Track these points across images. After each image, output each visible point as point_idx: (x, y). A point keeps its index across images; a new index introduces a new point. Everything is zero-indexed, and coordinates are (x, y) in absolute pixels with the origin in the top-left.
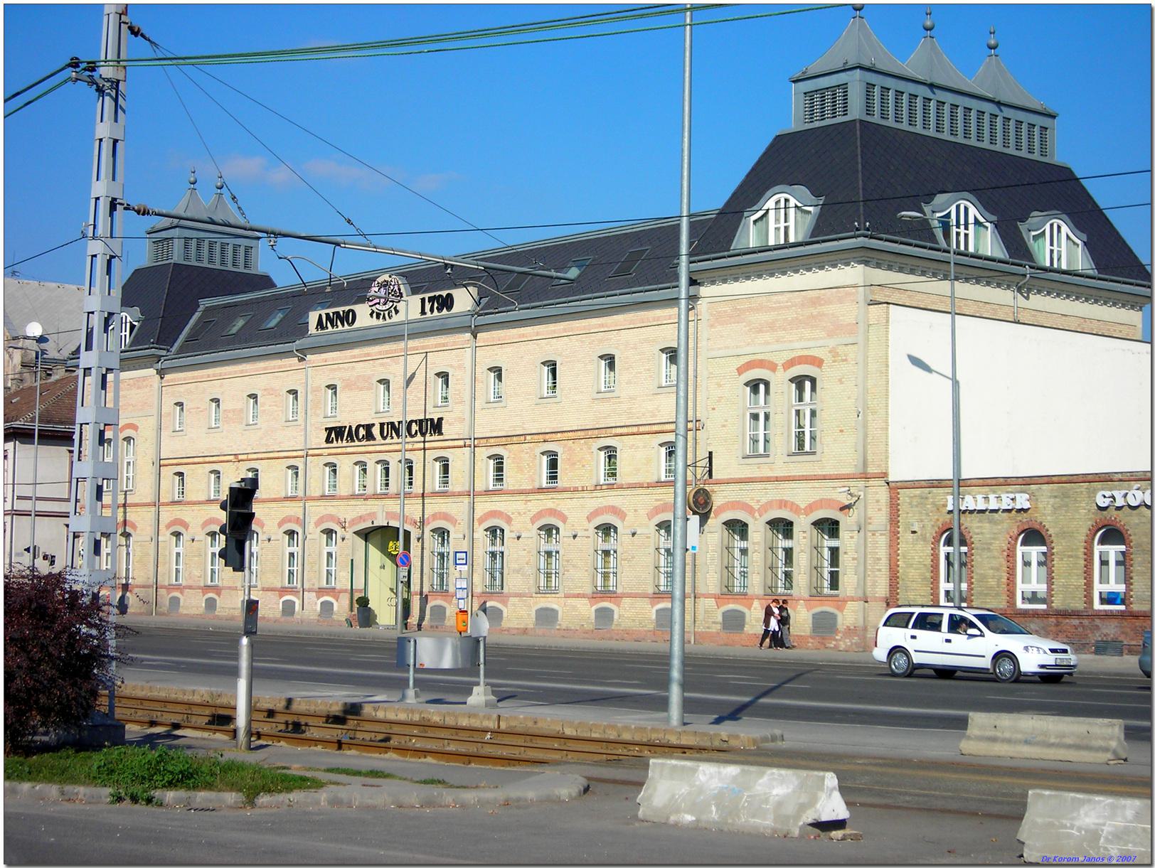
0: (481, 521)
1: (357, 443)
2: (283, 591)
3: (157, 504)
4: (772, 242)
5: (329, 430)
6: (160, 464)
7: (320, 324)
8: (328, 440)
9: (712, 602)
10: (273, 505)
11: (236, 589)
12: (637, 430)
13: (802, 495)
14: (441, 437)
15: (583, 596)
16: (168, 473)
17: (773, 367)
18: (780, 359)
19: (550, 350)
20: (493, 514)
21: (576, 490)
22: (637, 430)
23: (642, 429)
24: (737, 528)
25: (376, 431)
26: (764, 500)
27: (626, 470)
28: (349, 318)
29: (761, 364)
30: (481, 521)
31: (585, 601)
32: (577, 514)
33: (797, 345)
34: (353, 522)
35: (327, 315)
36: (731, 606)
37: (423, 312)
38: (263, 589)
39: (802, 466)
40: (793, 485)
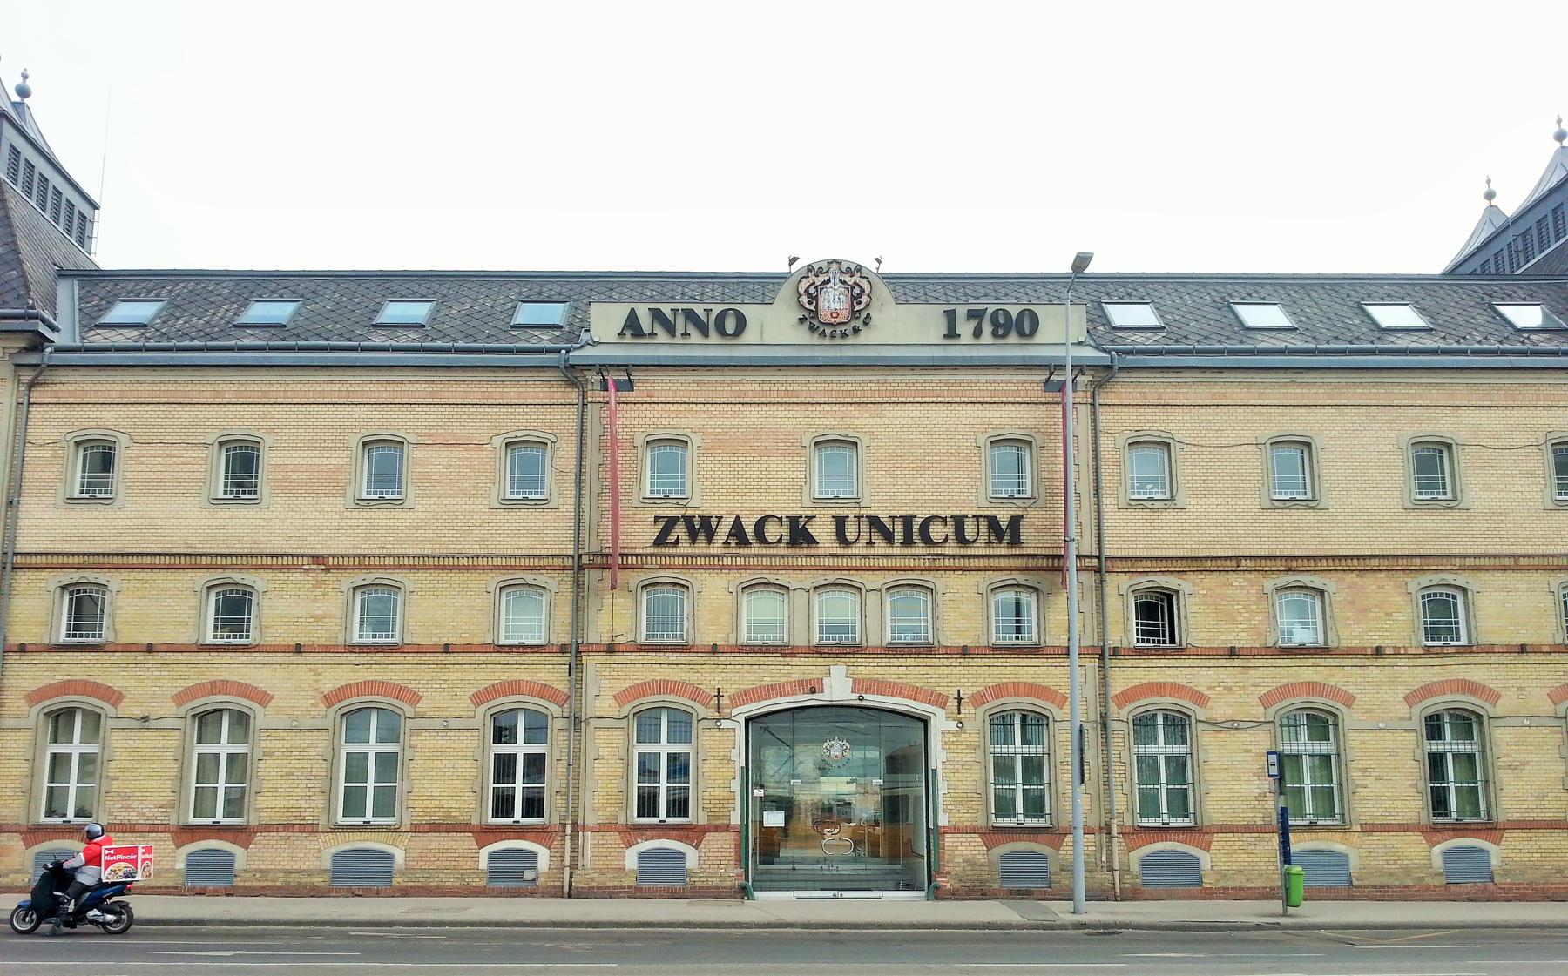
1: (756, 549)
8: (660, 541)
11: (310, 829)
12: (1513, 563)
14: (1017, 551)
15: (1405, 828)
22: (1513, 563)
23: (1522, 561)
25: (822, 531)
30: (1126, 697)
34: (743, 697)
35: (657, 315)
38: (416, 829)
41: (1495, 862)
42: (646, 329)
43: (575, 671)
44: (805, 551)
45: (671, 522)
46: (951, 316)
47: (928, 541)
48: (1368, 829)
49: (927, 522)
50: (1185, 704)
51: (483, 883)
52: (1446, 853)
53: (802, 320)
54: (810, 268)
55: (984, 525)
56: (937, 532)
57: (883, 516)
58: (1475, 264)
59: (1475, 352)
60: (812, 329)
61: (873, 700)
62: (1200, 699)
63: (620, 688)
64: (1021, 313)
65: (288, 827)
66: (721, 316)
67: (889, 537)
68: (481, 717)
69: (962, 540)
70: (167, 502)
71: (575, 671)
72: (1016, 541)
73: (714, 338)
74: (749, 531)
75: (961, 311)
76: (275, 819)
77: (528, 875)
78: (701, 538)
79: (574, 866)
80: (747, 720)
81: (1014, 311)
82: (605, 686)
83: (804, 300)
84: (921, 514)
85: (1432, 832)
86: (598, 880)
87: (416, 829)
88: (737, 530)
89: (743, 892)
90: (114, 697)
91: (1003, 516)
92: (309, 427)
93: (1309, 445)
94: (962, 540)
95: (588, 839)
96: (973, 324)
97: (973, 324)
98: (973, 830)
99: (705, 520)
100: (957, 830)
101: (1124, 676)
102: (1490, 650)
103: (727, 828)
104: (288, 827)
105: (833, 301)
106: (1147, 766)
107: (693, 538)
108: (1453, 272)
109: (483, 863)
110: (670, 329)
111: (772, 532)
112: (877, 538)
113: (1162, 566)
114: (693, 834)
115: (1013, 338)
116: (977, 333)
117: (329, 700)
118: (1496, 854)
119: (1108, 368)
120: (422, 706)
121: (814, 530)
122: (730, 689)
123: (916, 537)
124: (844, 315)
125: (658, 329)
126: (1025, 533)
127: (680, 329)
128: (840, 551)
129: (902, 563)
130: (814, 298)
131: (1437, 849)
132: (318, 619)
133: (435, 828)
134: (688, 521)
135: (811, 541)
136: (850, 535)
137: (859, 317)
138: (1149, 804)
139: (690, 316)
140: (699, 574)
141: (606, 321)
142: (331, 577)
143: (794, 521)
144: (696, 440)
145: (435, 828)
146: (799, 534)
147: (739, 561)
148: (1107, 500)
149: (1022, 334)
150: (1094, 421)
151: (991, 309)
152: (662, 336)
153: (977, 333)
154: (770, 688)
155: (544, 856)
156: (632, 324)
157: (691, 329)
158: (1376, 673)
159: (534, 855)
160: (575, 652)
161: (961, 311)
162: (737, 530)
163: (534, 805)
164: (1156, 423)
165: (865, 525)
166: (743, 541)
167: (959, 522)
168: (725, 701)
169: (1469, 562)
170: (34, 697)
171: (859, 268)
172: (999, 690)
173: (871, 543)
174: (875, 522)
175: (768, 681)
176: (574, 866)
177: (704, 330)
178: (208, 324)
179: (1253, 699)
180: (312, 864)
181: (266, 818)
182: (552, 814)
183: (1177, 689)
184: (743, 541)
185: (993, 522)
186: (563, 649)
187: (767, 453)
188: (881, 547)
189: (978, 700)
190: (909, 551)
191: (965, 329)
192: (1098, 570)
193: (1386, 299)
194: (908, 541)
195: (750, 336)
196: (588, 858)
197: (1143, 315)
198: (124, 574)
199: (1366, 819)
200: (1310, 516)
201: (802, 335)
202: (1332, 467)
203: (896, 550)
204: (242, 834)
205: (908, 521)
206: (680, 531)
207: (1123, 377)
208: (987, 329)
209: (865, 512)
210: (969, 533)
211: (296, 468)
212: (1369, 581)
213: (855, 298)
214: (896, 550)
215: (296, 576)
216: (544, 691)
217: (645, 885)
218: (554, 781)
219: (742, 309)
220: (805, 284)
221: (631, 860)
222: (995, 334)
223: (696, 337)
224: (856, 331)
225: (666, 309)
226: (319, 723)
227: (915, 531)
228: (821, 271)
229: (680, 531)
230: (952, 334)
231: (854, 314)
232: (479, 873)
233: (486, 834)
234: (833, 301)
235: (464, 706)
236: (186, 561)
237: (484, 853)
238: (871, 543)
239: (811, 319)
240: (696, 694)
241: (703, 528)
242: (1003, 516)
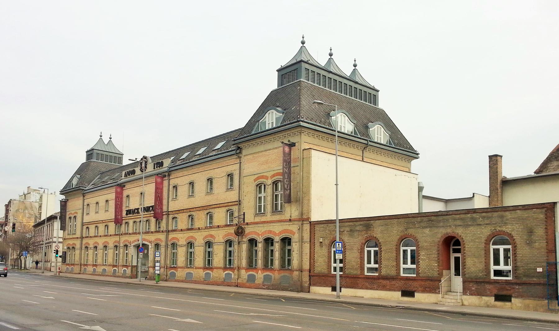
2: (114, 266)
3: (82, 238)
4: (267, 128)
5: (127, 211)
7: (126, 176)
8: (127, 214)
15: (200, 268)
16: (85, 227)
18: (269, 174)
20: (173, 238)
22: (219, 206)
24: (253, 242)
26: (263, 231)
27: (216, 222)
28: (133, 172)
29: (262, 177)
30: (171, 240)
31: (202, 270)
32: (199, 238)
33: (275, 169)
36: (251, 273)
37: (154, 168)
39: (277, 217)
85: (205, 268)
169: (213, 206)
200: (193, 198)
207: (172, 172)
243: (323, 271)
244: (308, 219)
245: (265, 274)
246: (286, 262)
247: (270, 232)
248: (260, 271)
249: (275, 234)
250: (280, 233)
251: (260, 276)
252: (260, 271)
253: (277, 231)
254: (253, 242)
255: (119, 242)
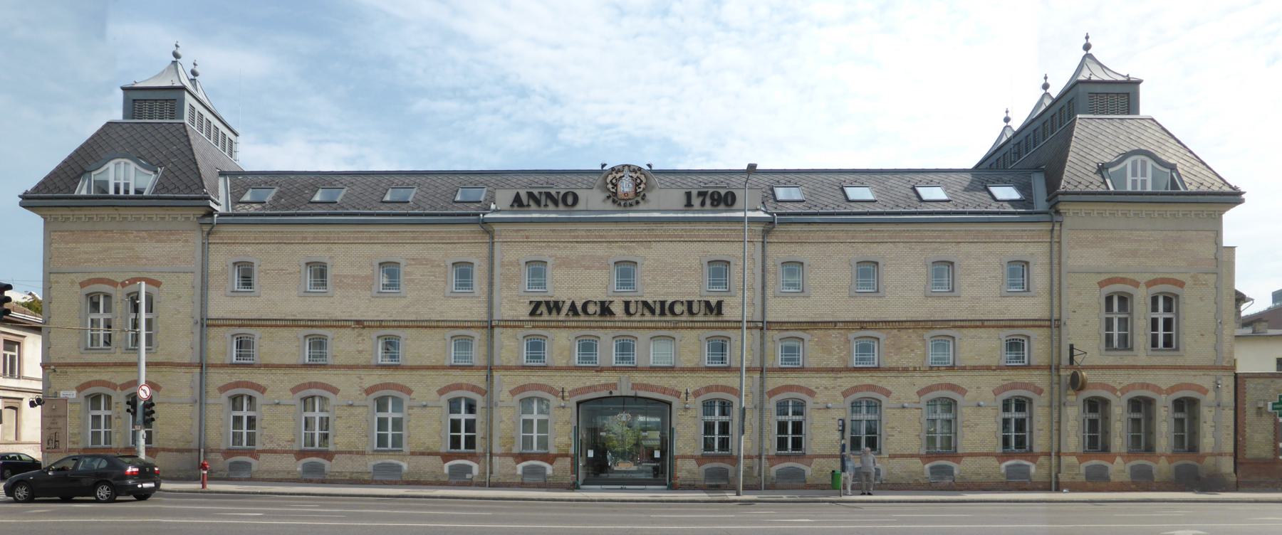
0: (773, 393)
1: (583, 317)
6: (206, 324)
8: (533, 313)
9: (1074, 460)
10: (431, 372)
13: (1164, 380)
17: (1136, 284)
19: (870, 252)
21: (906, 370)
24: (1095, 405)
25: (617, 308)
26: (1126, 383)
30: (773, 393)
35: (530, 195)
36: (1095, 462)
38: (413, 454)
39: (1166, 358)
40: (1157, 372)
41: (956, 472)
42: (525, 202)
43: (489, 378)
44: (608, 318)
45: (538, 304)
46: (689, 195)
47: (673, 313)
48: (893, 456)
49: (673, 304)
50: (803, 396)
51: (446, 479)
52: (931, 468)
53: (609, 197)
54: (613, 169)
55: (703, 305)
56: (678, 309)
57: (650, 301)
58: (986, 165)
59: (971, 213)
60: (614, 202)
61: (641, 394)
62: (811, 393)
63: (513, 387)
64: (727, 194)
65: (350, 452)
66: (565, 195)
67: (653, 312)
68: (444, 401)
69: (691, 312)
70: (282, 294)
71: (489, 378)
72: (719, 313)
73: (561, 207)
74: (579, 309)
75: (694, 193)
76: (344, 448)
77: (468, 476)
78: (554, 312)
79: (491, 473)
80: (578, 403)
81: (723, 192)
82: (504, 383)
83: (610, 186)
84: (670, 300)
85: (928, 457)
86: (502, 480)
87: (413, 454)
88: (573, 307)
89: (574, 487)
90: (262, 390)
91: (713, 301)
92: (352, 255)
93: (877, 263)
94: (691, 312)
95: (495, 459)
96: (701, 199)
97: (701, 199)
98: (692, 457)
99: (556, 303)
100: (683, 457)
101: (773, 382)
102: (964, 368)
103: (567, 455)
104: (350, 452)
105: (626, 187)
106: (782, 427)
107: (550, 312)
108: (977, 167)
109: (446, 470)
110: (538, 202)
111: (591, 309)
112: (646, 312)
113: (796, 326)
114: (550, 459)
115: (722, 207)
116: (703, 204)
117: (368, 391)
118: (957, 469)
119: (772, 223)
120: (413, 395)
121: (613, 308)
122: (569, 388)
123: (667, 311)
124: (631, 195)
125: (532, 203)
126: (725, 310)
127: (543, 203)
128: (626, 318)
129: (660, 325)
130: (615, 185)
131: (927, 466)
132: (360, 352)
133: (422, 454)
134: (547, 303)
135: (612, 313)
136: (632, 310)
137: (639, 196)
138: (782, 444)
139: (548, 195)
140: (552, 331)
141: (504, 197)
142: (365, 331)
143: (603, 303)
144: (550, 262)
145: (422, 454)
146: (605, 309)
147: (574, 324)
148: (769, 292)
149: (727, 204)
150: (763, 251)
151: (711, 191)
152: (533, 206)
153: (703, 204)
154: (589, 388)
155: (476, 468)
156: (517, 201)
157: (549, 202)
158: (903, 380)
159: (471, 467)
160: (490, 369)
161: (694, 193)
162: (573, 307)
163: (471, 442)
164: (798, 253)
165: (640, 306)
166: (576, 313)
167: (690, 303)
168: (566, 394)
170: (223, 389)
171: (640, 169)
172: (708, 389)
173: (643, 315)
174: (645, 304)
175: (588, 384)
176: (491, 473)
177: (556, 203)
178: (295, 201)
179: (838, 393)
180: (362, 469)
181: (339, 448)
182: (479, 449)
183: (799, 389)
184: (576, 313)
185: (708, 303)
186: (485, 368)
187: (588, 268)
188: (648, 317)
189: (697, 394)
190: (663, 318)
191: (696, 202)
192: (762, 329)
193: (929, 184)
194: (663, 313)
195: (580, 206)
196: (496, 468)
197: (795, 194)
198: (263, 329)
199: (892, 452)
200: (875, 301)
201: (609, 205)
202: (889, 276)
203: (657, 318)
204: (328, 455)
205: (663, 303)
206: (543, 309)
208: (708, 202)
209: (640, 299)
210: (695, 309)
211: (345, 276)
212: (904, 335)
213: (637, 185)
214: (657, 318)
215: (348, 331)
216: (474, 388)
217: (527, 480)
218: (479, 433)
219: (577, 192)
220: (610, 178)
221: (520, 467)
222: (712, 204)
223: (551, 207)
224: (637, 203)
225: (536, 192)
226: (363, 403)
227: (666, 308)
228: (618, 171)
229: (543, 309)
230: (689, 204)
231: (637, 194)
232: (444, 475)
233: (446, 457)
234: (626, 187)
235: (434, 395)
236: (294, 323)
237: (447, 465)
238: (643, 315)
239: (614, 197)
240: (551, 390)
241: (555, 307)
242: (713, 301)
243: (1263, 455)
244: (1233, 368)
245: (1134, 463)
246: (1187, 439)
247: (1189, 386)
248: (1119, 460)
249: (1158, 390)
250: (1172, 389)
251: (1119, 468)
252: (1119, 460)
253: (1164, 383)
254: (1095, 405)
255: (487, 392)
